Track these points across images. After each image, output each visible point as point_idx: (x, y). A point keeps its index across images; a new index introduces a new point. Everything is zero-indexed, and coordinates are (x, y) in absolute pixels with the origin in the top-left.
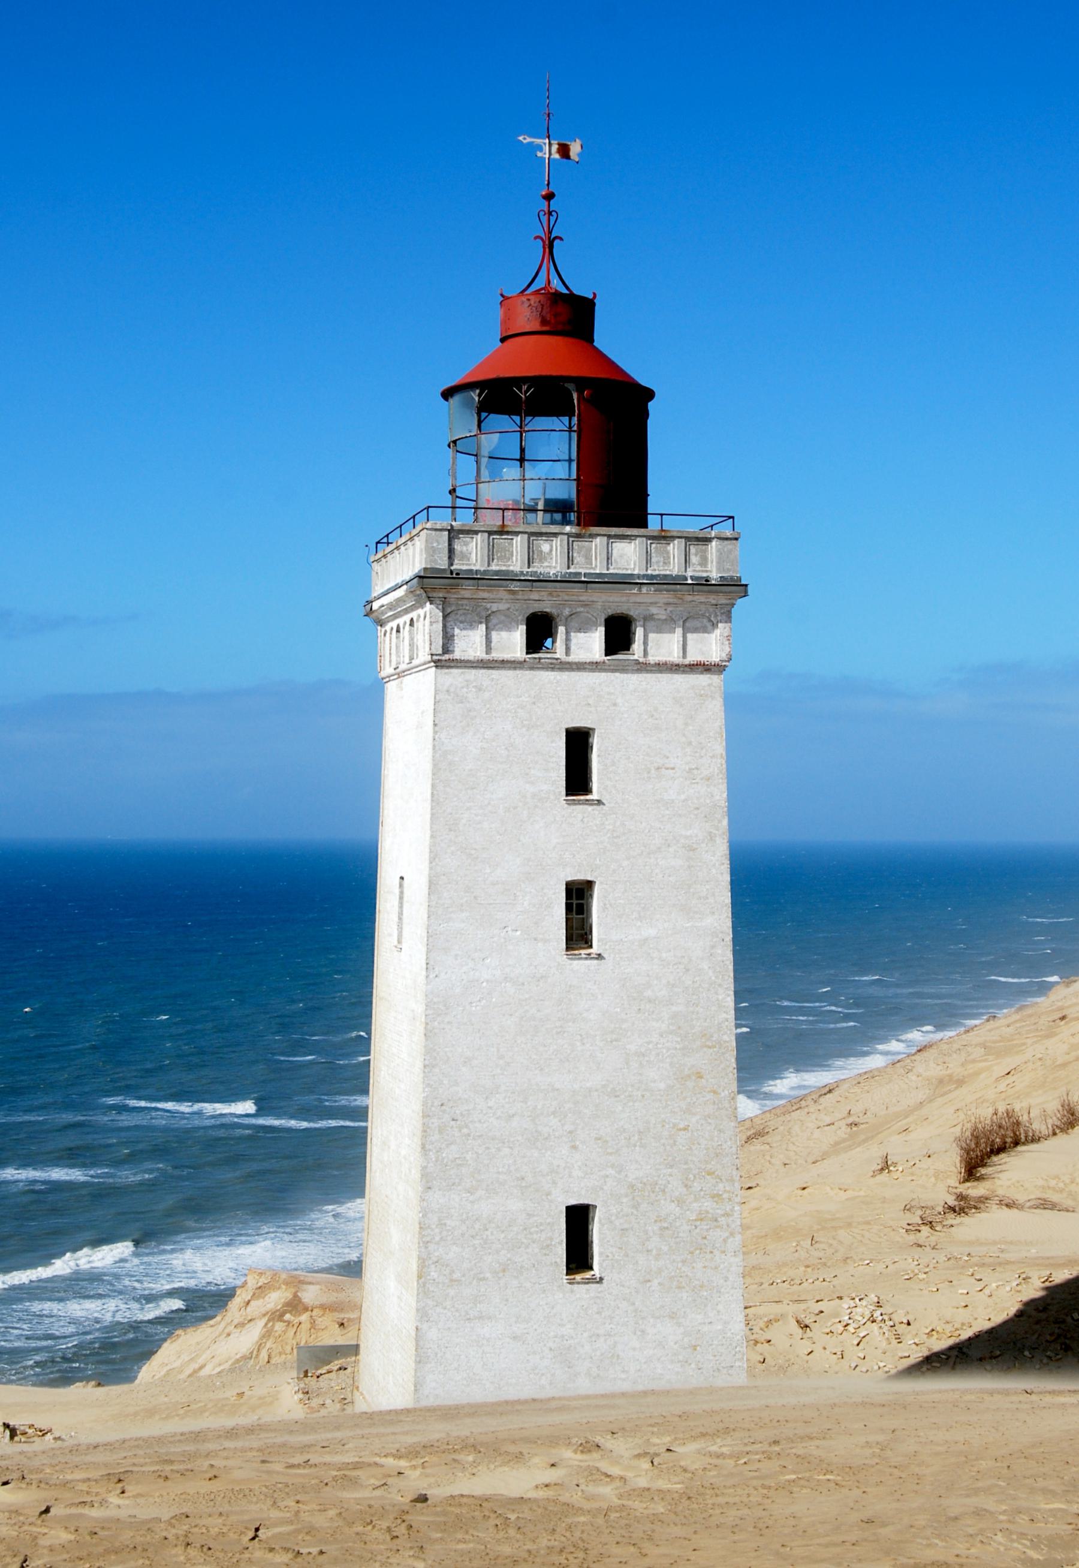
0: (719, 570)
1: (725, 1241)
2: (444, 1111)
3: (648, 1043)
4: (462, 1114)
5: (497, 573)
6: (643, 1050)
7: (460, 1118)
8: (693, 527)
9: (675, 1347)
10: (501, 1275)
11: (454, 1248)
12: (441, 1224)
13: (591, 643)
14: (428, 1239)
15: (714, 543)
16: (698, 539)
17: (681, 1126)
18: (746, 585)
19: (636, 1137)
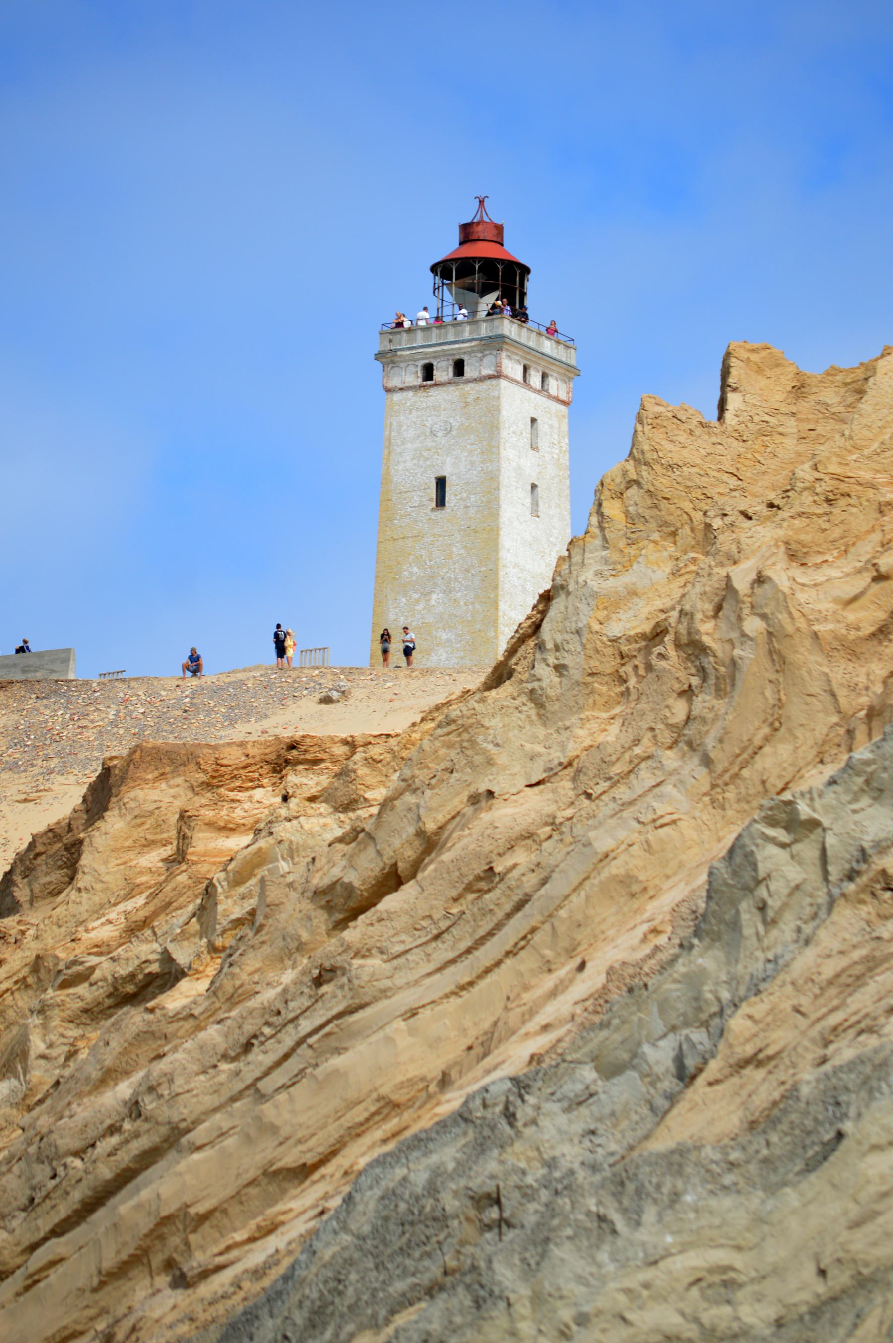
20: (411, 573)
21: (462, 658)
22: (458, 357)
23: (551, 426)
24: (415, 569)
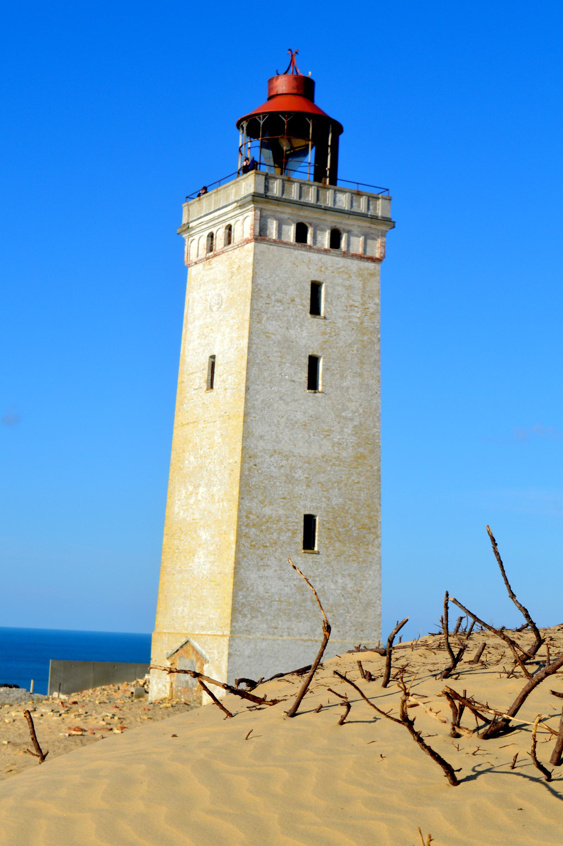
0: (382, 213)
1: (374, 539)
2: (251, 461)
3: (343, 438)
4: (259, 463)
5: (285, 199)
6: (340, 442)
7: (258, 465)
8: (374, 192)
9: (351, 590)
10: (274, 545)
11: (253, 530)
12: (247, 517)
13: (325, 240)
14: (242, 523)
15: (380, 200)
16: (373, 197)
17: (356, 481)
18: (394, 222)
19: (336, 484)
20: (189, 462)
21: (213, 563)
22: (228, 223)
23: (350, 288)
24: (192, 459)
